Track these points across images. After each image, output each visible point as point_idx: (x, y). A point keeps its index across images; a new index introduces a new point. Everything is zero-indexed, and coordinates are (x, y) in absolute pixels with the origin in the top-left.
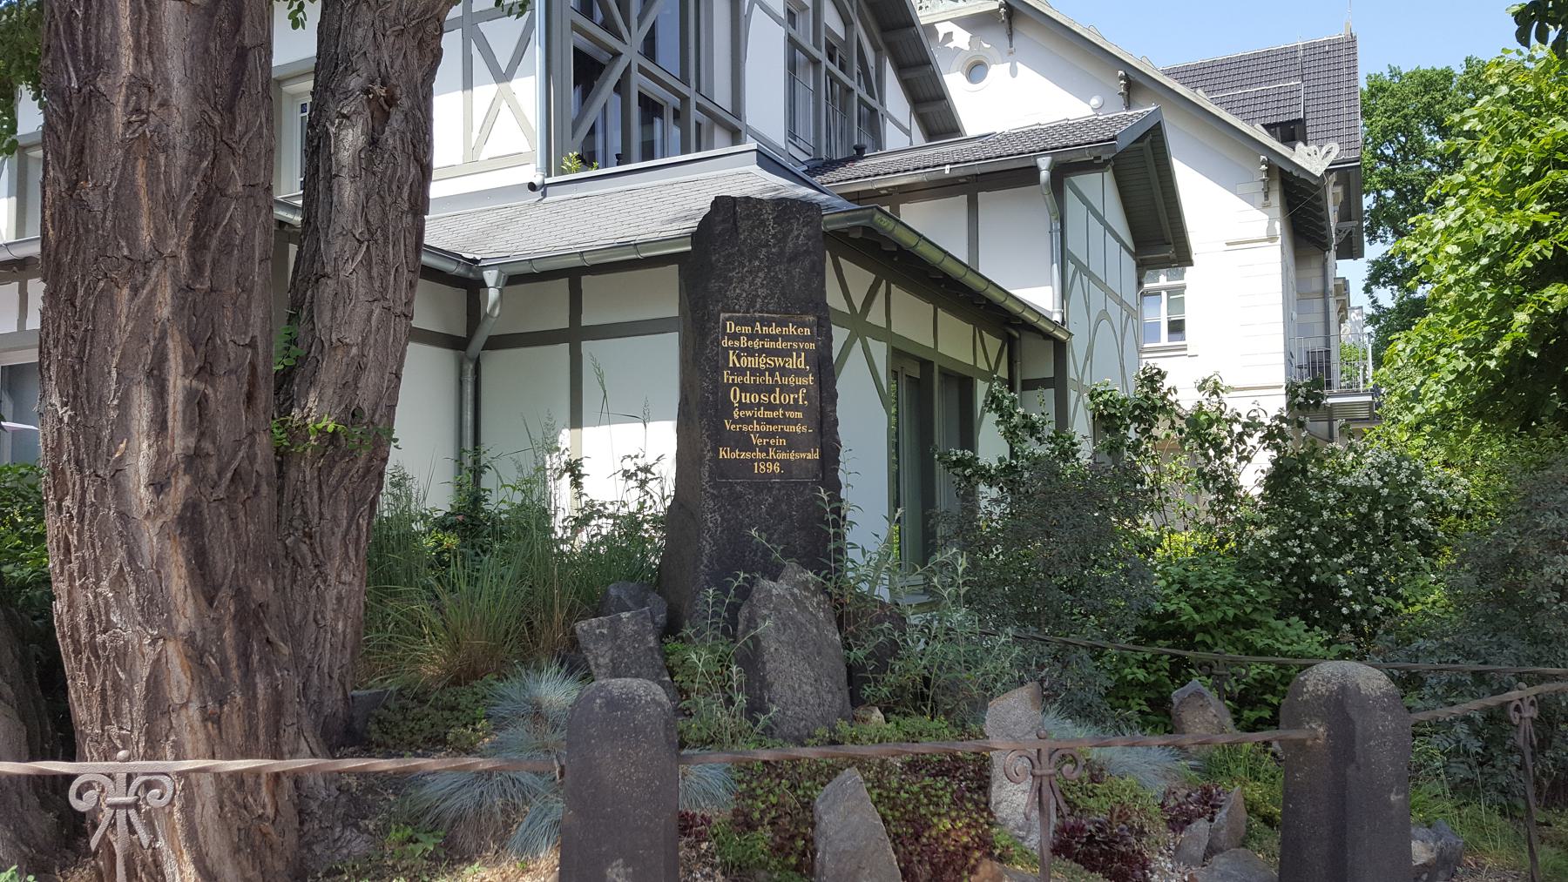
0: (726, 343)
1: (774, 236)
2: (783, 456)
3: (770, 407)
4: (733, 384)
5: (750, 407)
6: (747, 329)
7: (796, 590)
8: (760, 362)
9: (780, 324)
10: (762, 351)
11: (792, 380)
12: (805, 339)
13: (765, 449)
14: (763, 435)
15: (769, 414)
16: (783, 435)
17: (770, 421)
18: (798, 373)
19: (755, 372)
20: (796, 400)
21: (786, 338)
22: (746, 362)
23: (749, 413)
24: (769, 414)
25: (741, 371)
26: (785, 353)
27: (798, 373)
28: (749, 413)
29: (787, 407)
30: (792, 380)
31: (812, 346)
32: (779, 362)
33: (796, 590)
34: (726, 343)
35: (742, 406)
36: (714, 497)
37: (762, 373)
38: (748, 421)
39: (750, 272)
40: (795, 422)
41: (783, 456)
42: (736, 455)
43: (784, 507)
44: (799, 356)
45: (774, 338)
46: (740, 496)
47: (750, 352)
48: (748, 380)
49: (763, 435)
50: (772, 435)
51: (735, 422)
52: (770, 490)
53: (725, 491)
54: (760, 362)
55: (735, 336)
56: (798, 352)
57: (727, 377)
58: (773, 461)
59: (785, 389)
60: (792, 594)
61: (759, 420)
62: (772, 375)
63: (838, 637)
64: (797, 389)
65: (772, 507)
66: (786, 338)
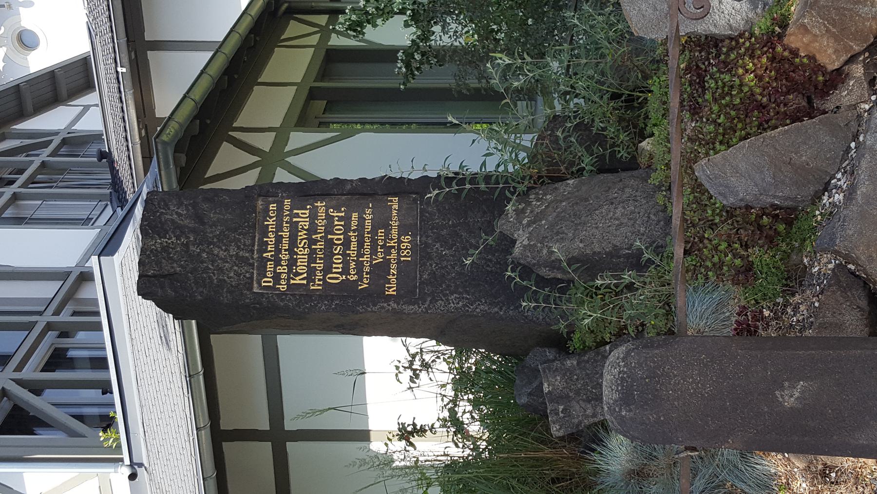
0: (283, 287)
2: (394, 233)
3: (346, 244)
4: (324, 280)
6: (270, 266)
7: (525, 222)
8: (302, 252)
9: (265, 233)
11: (321, 223)
12: (280, 209)
13: (387, 250)
14: (374, 251)
15: (354, 245)
16: (374, 231)
17: (361, 244)
18: (313, 216)
19: (312, 258)
20: (340, 219)
21: (279, 227)
24: (354, 245)
25: (311, 272)
26: (294, 228)
27: (313, 216)
30: (321, 223)
31: (287, 202)
32: (302, 234)
33: (525, 222)
34: (283, 287)
35: (345, 271)
37: (313, 252)
39: (213, 262)
40: (361, 220)
41: (394, 233)
43: (444, 232)
44: (297, 215)
45: (279, 239)
46: (433, 274)
47: (292, 263)
48: (319, 265)
49: (374, 251)
51: (361, 279)
54: (302, 252)
55: (277, 277)
56: (292, 216)
58: (400, 242)
60: (529, 224)
62: (315, 242)
63: (571, 182)
64: (329, 218)
66: (279, 227)
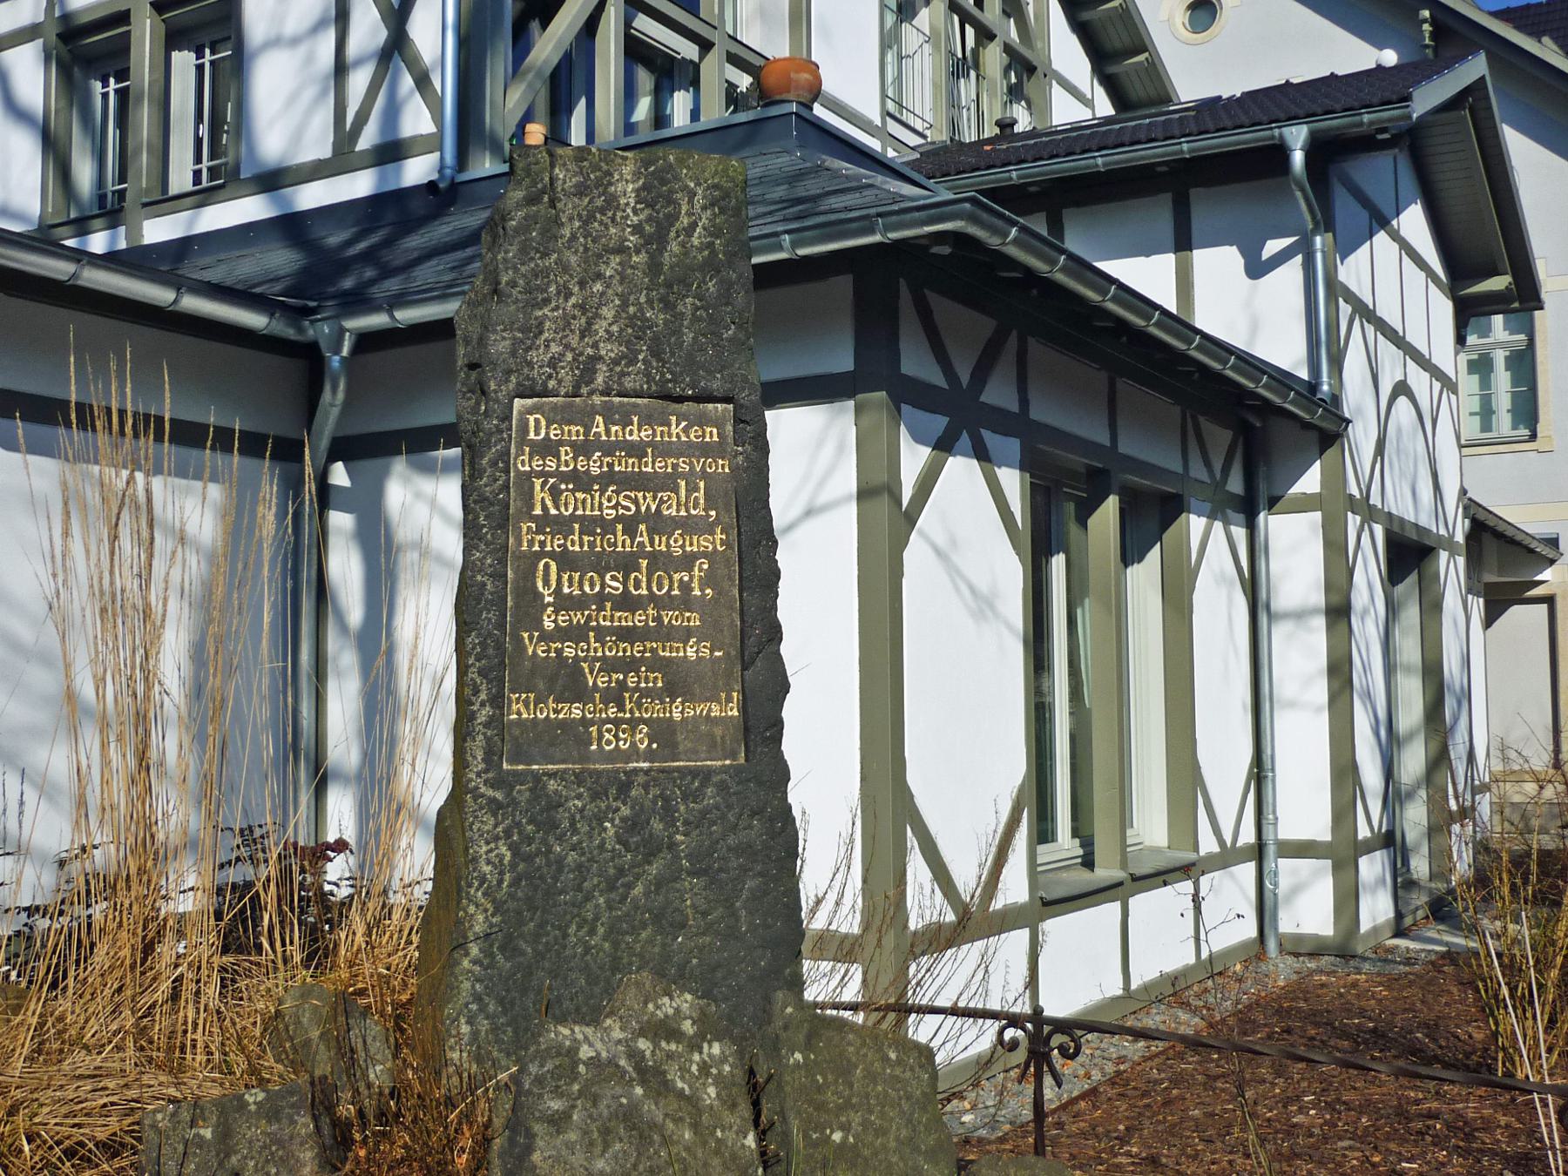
0: (524, 464)
1: (637, 229)
2: (654, 710)
3: (627, 602)
4: (542, 554)
5: (580, 603)
6: (575, 431)
7: (643, 1044)
8: (608, 504)
9: (648, 420)
10: (608, 478)
11: (676, 544)
12: (705, 450)
13: (615, 696)
14: (609, 666)
15: (624, 619)
16: (657, 664)
17: (627, 635)
18: (690, 526)
19: (590, 525)
20: (686, 587)
21: (664, 451)
22: (573, 504)
23: (578, 618)
24: (624, 619)
25: (561, 526)
26: (666, 483)
27: (690, 526)
28: (578, 618)
29: (661, 603)
30: (676, 544)
31: (722, 466)
32: (648, 503)
33: (643, 1044)
34: (524, 464)
35: (564, 603)
36: (495, 807)
37: (608, 527)
38: (575, 634)
39: (582, 307)
40: (686, 635)
41: (654, 710)
42: (546, 712)
43: (657, 825)
44: (691, 488)
45: (637, 450)
46: (557, 804)
47: (581, 481)
48: (576, 544)
49: (609, 666)
50: (630, 665)
51: (546, 637)
52: (624, 788)
53: (522, 792)
54: (608, 504)
55: (547, 448)
56: (690, 478)
57: (526, 538)
58: (633, 724)
59: (660, 562)
60: (635, 1055)
61: (601, 634)
62: (631, 531)
63: (750, 1141)
64: (688, 561)
65: (633, 825)
66: (664, 451)
